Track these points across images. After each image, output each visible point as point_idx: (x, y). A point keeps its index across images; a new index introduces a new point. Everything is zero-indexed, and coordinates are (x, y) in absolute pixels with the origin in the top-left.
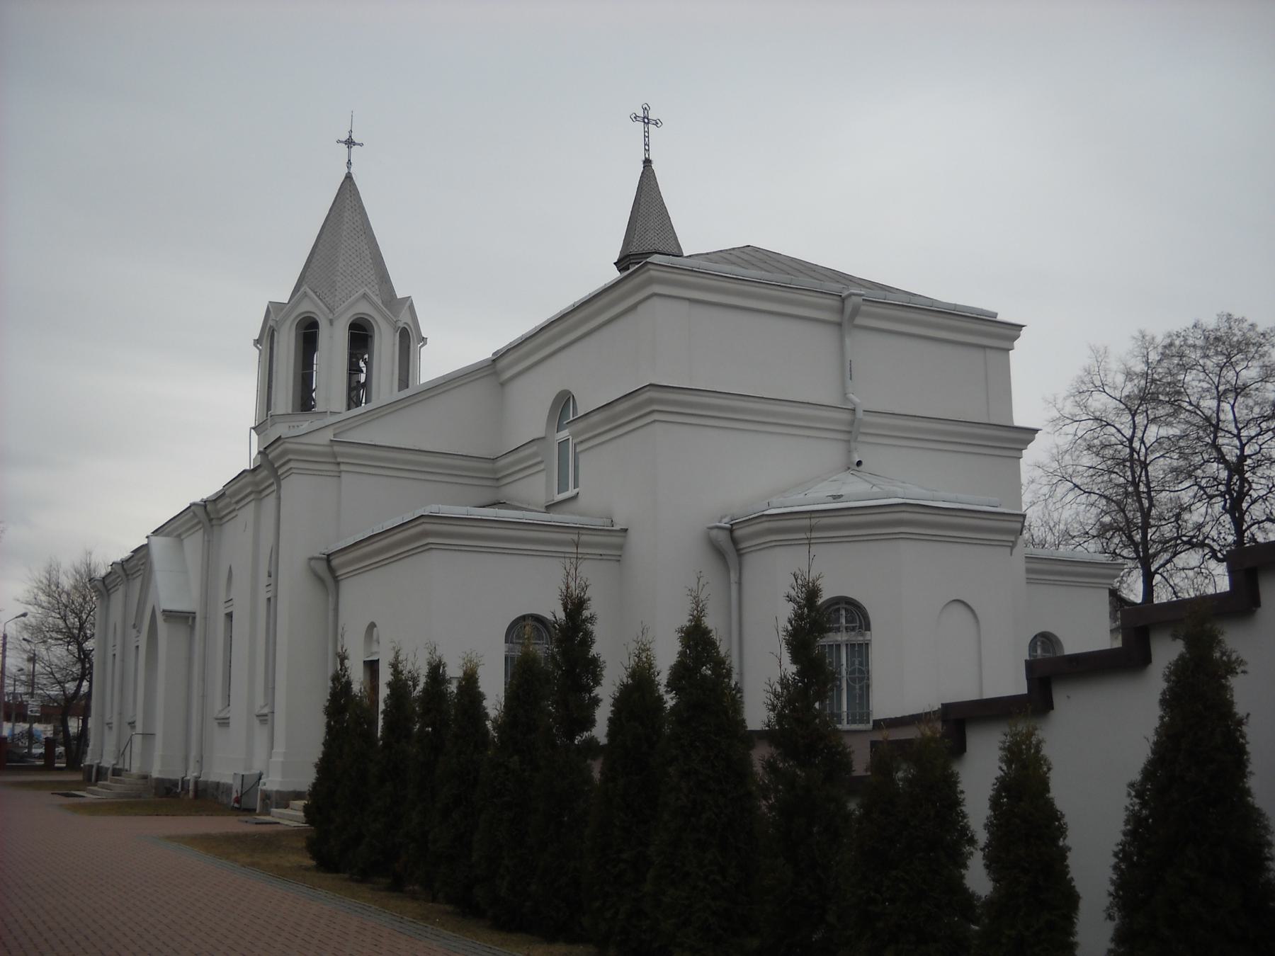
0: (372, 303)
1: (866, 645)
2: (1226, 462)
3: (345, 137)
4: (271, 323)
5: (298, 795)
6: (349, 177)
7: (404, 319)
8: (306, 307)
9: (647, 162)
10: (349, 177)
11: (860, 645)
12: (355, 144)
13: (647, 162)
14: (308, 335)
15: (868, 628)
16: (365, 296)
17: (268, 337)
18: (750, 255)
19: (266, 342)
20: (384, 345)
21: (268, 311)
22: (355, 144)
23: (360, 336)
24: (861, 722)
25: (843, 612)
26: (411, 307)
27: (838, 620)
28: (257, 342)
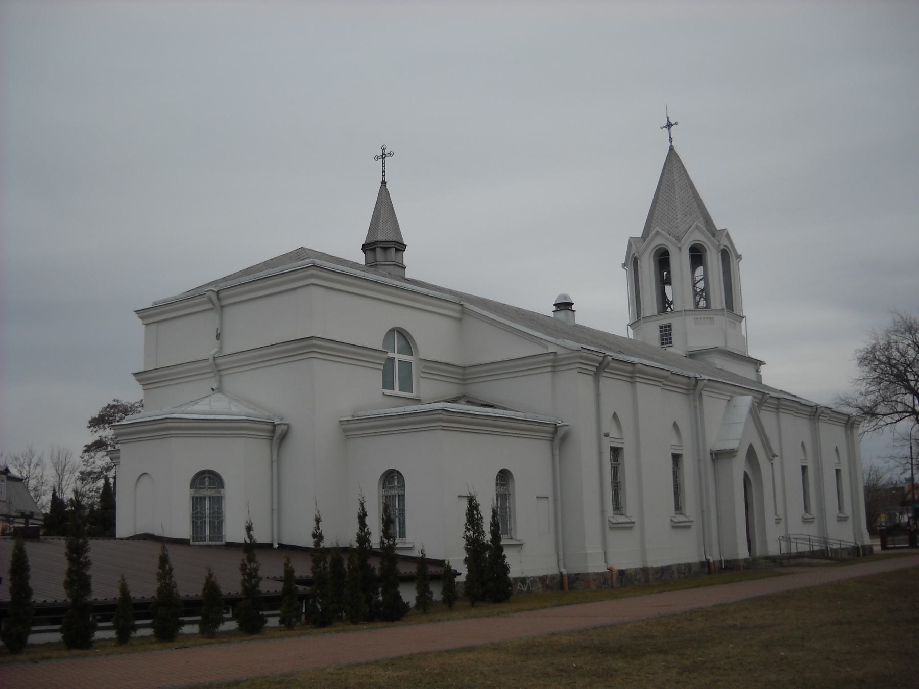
0: (663, 236)
1: (403, 495)
2: (884, 363)
3: (672, 121)
4: (633, 250)
5: (164, 547)
6: (672, 149)
7: (725, 242)
8: (659, 241)
9: (384, 183)
10: (672, 149)
11: (201, 498)
12: (672, 125)
13: (384, 183)
14: (663, 259)
15: (223, 487)
16: (657, 233)
17: (633, 262)
18: (300, 253)
19: (631, 264)
20: (713, 259)
21: (630, 245)
22: (666, 126)
23: (697, 256)
24: (218, 540)
25: (207, 479)
26: (728, 236)
27: (204, 484)
28: (624, 265)
